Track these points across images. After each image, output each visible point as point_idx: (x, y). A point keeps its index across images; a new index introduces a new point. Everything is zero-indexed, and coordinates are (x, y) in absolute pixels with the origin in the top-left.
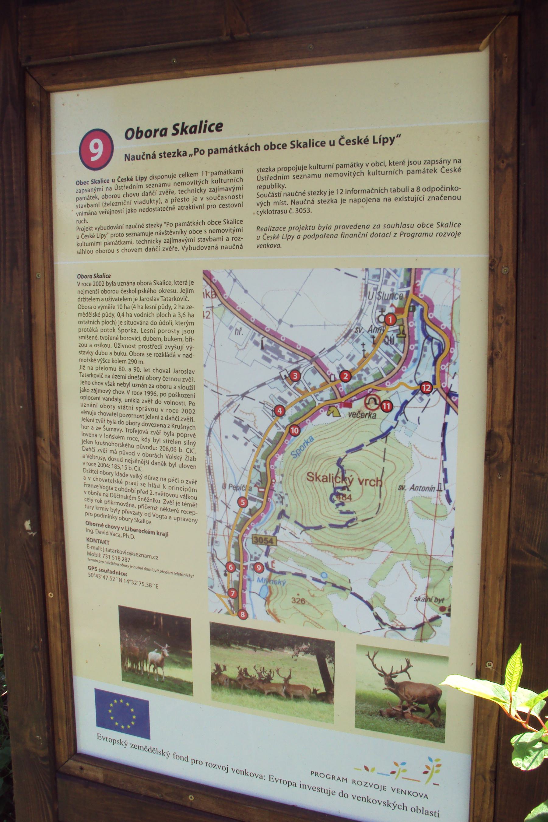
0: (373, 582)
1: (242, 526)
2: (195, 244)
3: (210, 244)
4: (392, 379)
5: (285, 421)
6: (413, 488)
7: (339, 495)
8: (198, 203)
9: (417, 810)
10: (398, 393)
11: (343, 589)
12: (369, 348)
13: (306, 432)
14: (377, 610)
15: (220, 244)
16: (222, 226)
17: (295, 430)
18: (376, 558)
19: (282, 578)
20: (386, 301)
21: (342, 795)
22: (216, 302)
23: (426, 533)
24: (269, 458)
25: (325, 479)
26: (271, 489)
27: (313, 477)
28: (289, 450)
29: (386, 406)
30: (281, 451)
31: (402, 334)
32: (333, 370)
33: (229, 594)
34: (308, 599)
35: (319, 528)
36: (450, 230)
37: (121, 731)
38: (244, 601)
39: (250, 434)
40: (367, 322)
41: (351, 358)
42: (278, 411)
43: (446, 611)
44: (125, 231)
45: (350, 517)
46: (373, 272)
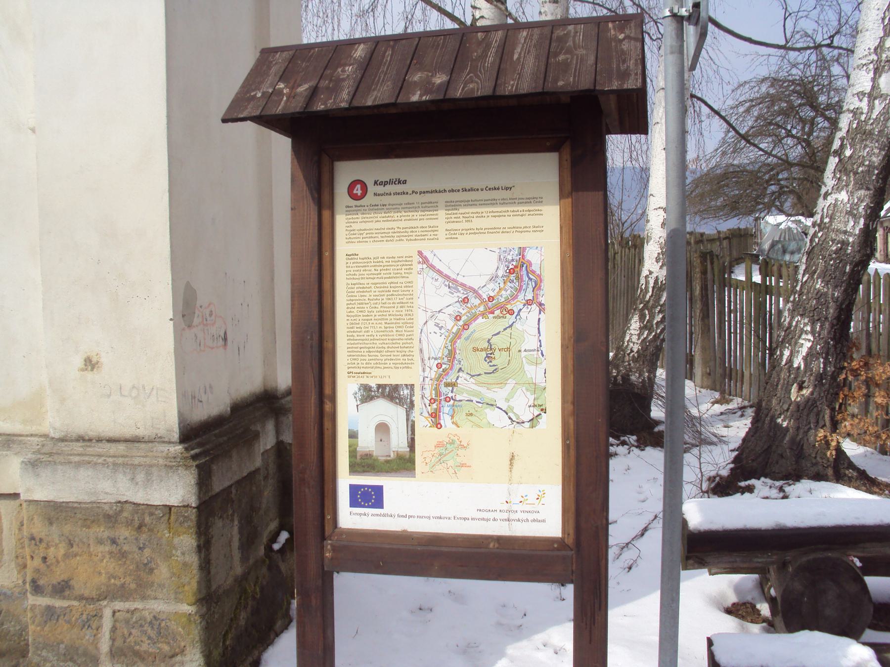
0: (507, 400)
1: (439, 378)
2: (414, 238)
3: (422, 238)
4: (513, 299)
5: (461, 323)
6: (525, 351)
7: (489, 358)
8: (415, 218)
9: (534, 520)
10: (516, 306)
11: (492, 405)
12: (502, 285)
13: (473, 326)
14: (510, 414)
15: (426, 237)
16: (427, 229)
17: (466, 327)
18: (508, 387)
19: (460, 403)
20: (509, 262)
21: (494, 520)
22: (425, 266)
23: (533, 373)
24: (453, 342)
25: (482, 350)
26: (454, 358)
27: (475, 350)
28: (463, 337)
29: (511, 312)
30: (459, 338)
31: (517, 278)
32: (485, 296)
33: (431, 415)
34: (474, 413)
35: (479, 375)
36: (538, 229)
37: (364, 506)
38: (440, 419)
39: (443, 331)
40: (501, 273)
41: (493, 290)
42: (458, 318)
43: (544, 410)
44: (374, 231)
45: (494, 368)
46: (503, 249)
